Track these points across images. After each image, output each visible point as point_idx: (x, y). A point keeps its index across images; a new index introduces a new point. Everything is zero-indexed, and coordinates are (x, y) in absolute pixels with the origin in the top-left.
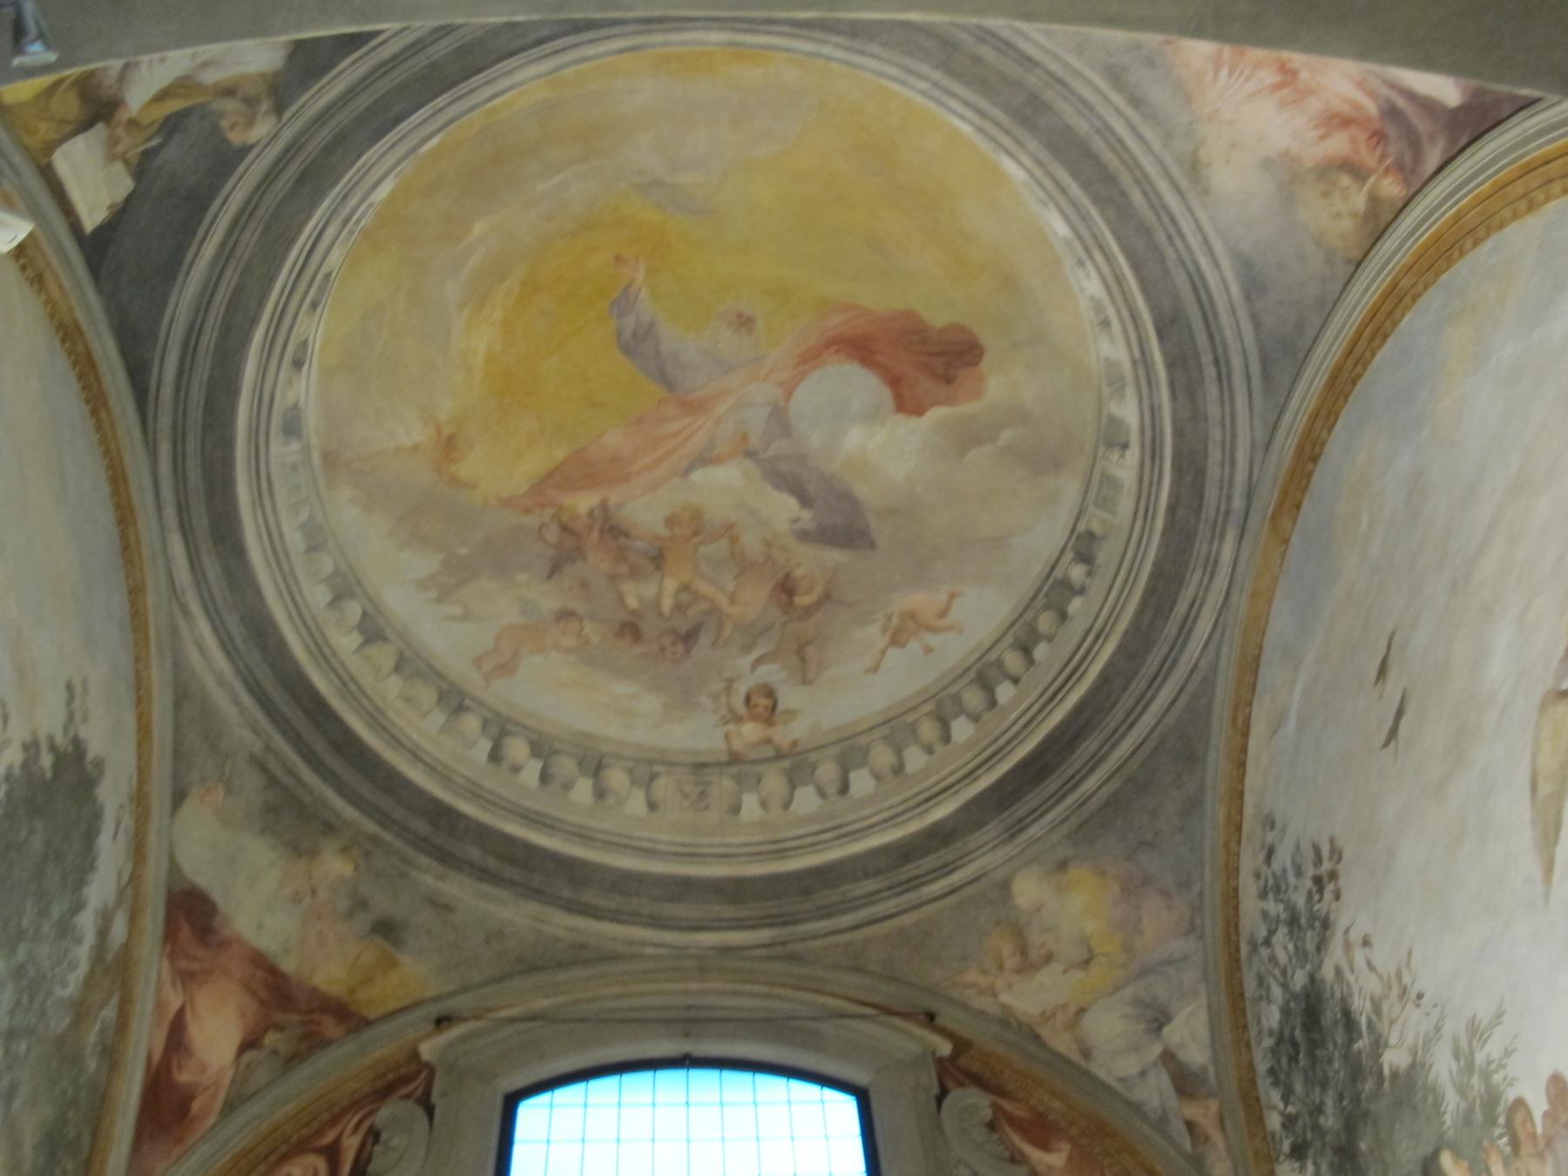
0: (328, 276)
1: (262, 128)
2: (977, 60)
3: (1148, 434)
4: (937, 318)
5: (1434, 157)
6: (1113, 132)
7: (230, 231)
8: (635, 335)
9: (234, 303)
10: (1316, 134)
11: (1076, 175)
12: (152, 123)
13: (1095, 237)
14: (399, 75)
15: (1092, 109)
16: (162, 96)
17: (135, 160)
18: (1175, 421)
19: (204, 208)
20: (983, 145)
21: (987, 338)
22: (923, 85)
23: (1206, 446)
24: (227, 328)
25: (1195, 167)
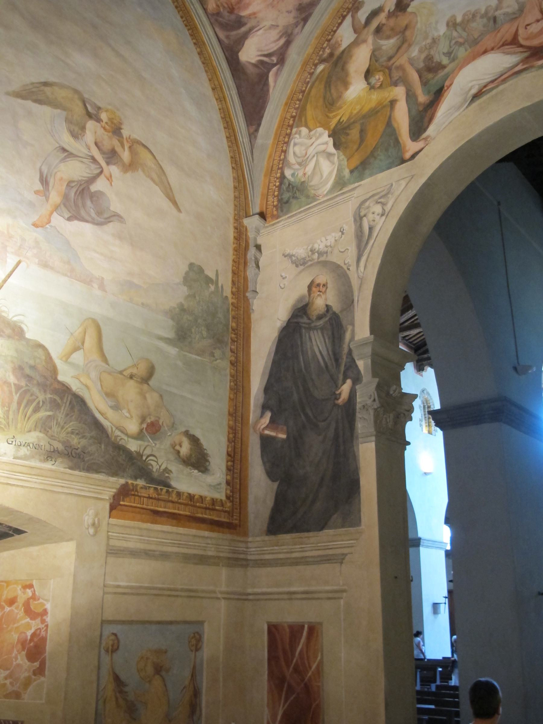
5: (222, 35)
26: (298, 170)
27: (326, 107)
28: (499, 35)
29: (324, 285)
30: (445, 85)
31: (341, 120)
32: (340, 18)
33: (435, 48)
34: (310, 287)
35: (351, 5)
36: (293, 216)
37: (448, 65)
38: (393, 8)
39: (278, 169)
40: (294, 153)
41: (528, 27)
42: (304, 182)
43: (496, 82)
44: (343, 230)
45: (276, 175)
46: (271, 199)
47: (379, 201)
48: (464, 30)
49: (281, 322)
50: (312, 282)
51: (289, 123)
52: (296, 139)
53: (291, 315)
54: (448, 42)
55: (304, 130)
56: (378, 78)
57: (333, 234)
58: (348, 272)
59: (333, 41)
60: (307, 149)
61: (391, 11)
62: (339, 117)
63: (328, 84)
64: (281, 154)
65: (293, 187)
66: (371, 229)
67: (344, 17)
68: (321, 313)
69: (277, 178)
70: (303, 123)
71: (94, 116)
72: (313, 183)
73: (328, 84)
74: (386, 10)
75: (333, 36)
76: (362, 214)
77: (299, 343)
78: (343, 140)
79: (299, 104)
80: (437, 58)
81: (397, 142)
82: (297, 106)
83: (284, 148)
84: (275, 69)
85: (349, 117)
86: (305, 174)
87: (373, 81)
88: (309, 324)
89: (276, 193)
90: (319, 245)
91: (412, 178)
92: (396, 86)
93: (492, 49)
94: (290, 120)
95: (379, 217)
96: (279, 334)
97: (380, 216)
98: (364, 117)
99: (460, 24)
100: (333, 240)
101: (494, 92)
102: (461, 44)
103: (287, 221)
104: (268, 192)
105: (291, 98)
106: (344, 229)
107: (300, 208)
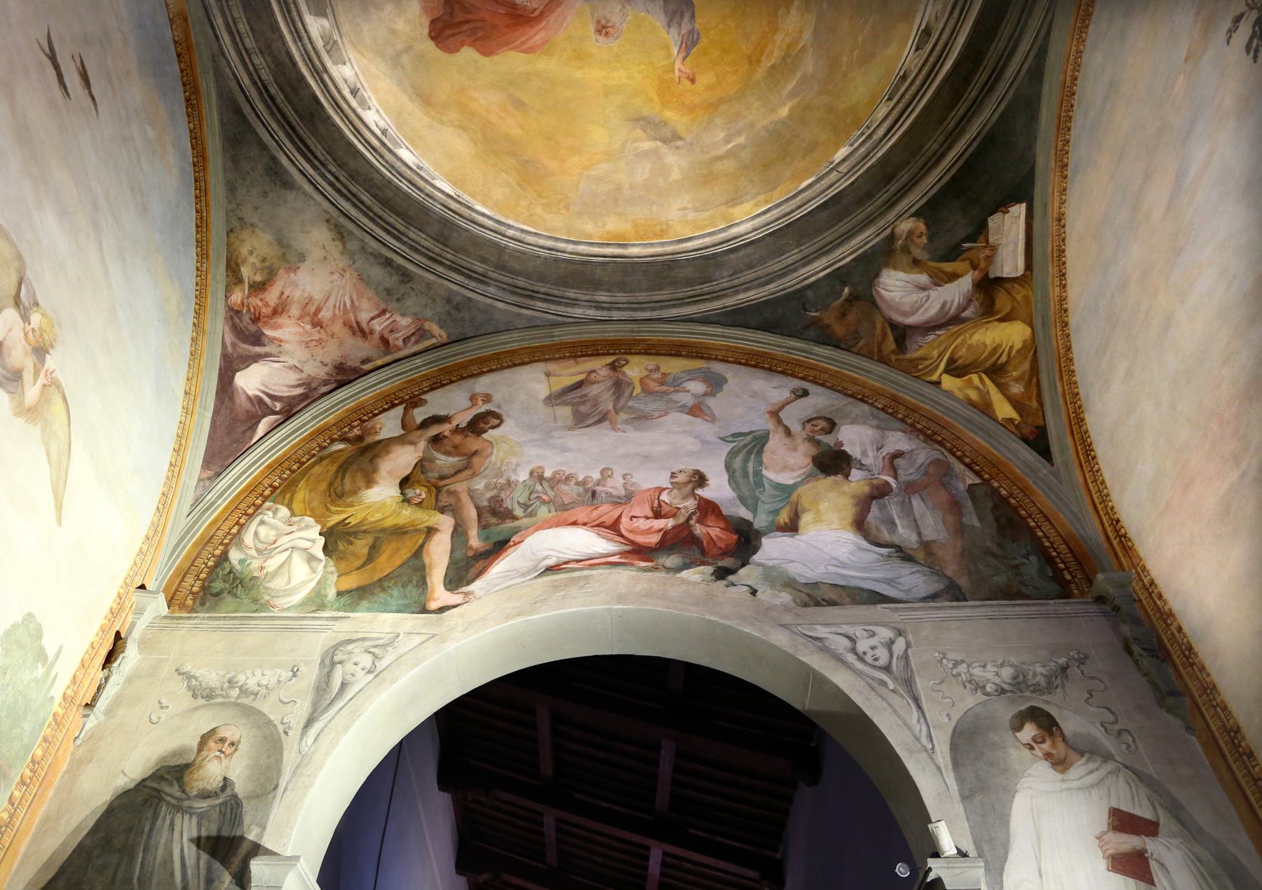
0: (890, 99)
1: (905, 226)
2: (484, 260)
3: (295, 14)
4: (468, 54)
6: (395, 237)
7: (943, 155)
8: (682, 14)
9: (957, 96)
10: (287, 293)
11: (407, 195)
12: (963, 260)
13: (382, 157)
14: (820, 241)
15: (411, 247)
16: (953, 277)
17: (982, 238)
18: (282, 37)
19: (953, 179)
20: (466, 198)
21: (430, 46)
22: (511, 232)
23: (252, 29)
24: (967, 81)
25: (341, 235)
26: (254, 558)
27: (330, 496)
28: (596, 513)
29: (232, 744)
30: (512, 539)
31: (347, 521)
32: (387, 403)
33: (508, 493)
34: (204, 740)
35: (407, 397)
36: (219, 618)
37: (522, 518)
38: (464, 425)
39: (221, 544)
40: (256, 533)
41: (634, 520)
42: (254, 578)
43: (583, 563)
44: (298, 670)
45: (214, 550)
46: (190, 580)
47: (371, 650)
48: (552, 488)
49: (126, 779)
50: (213, 731)
51: (263, 491)
52: (268, 516)
53: (150, 773)
54: (528, 493)
55: (284, 511)
56: (419, 492)
57: (278, 671)
58: (283, 735)
59: (369, 424)
60: (279, 536)
61: (460, 426)
62: (343, 516)
63: (343, 469)
64: (234, 526)
65: (235, 578)
66: (344, 685)
67: (394, 406)
68: (209, 787)
69: (213, 556)
70: (286, 502)
71: (21, 307)
72: (272, 585)
73: (343, 469)
74: (455, 423)
75: (370, 418)
76: (337, 658)
77: (147, 829)
78: (341, 547)
79: (289, 476)
80: (508, 504)
81: (423, 583)
82: (286, 476)
83: (242, 521)
84: (272, 418)
85: (361, 522)
86: (262, 568)
87: (410, 493)
88: (179, 799)
89: (203, 576)
90: (247, 678)
91: (432, 637)
92: (442, 513)
93: (585, 524)
94: (266, 488)
95: (364, 672)
96: (113, 798)
97: (365, 671)
98: (383, 530)
99: (550, 480)
100: (274, 680)
101: (576, 574)
102: (544, 502)
103: (205, 622)
104: (189, 569)
105: (280, 463)
106: (300, 669)
107: (236, 611)
